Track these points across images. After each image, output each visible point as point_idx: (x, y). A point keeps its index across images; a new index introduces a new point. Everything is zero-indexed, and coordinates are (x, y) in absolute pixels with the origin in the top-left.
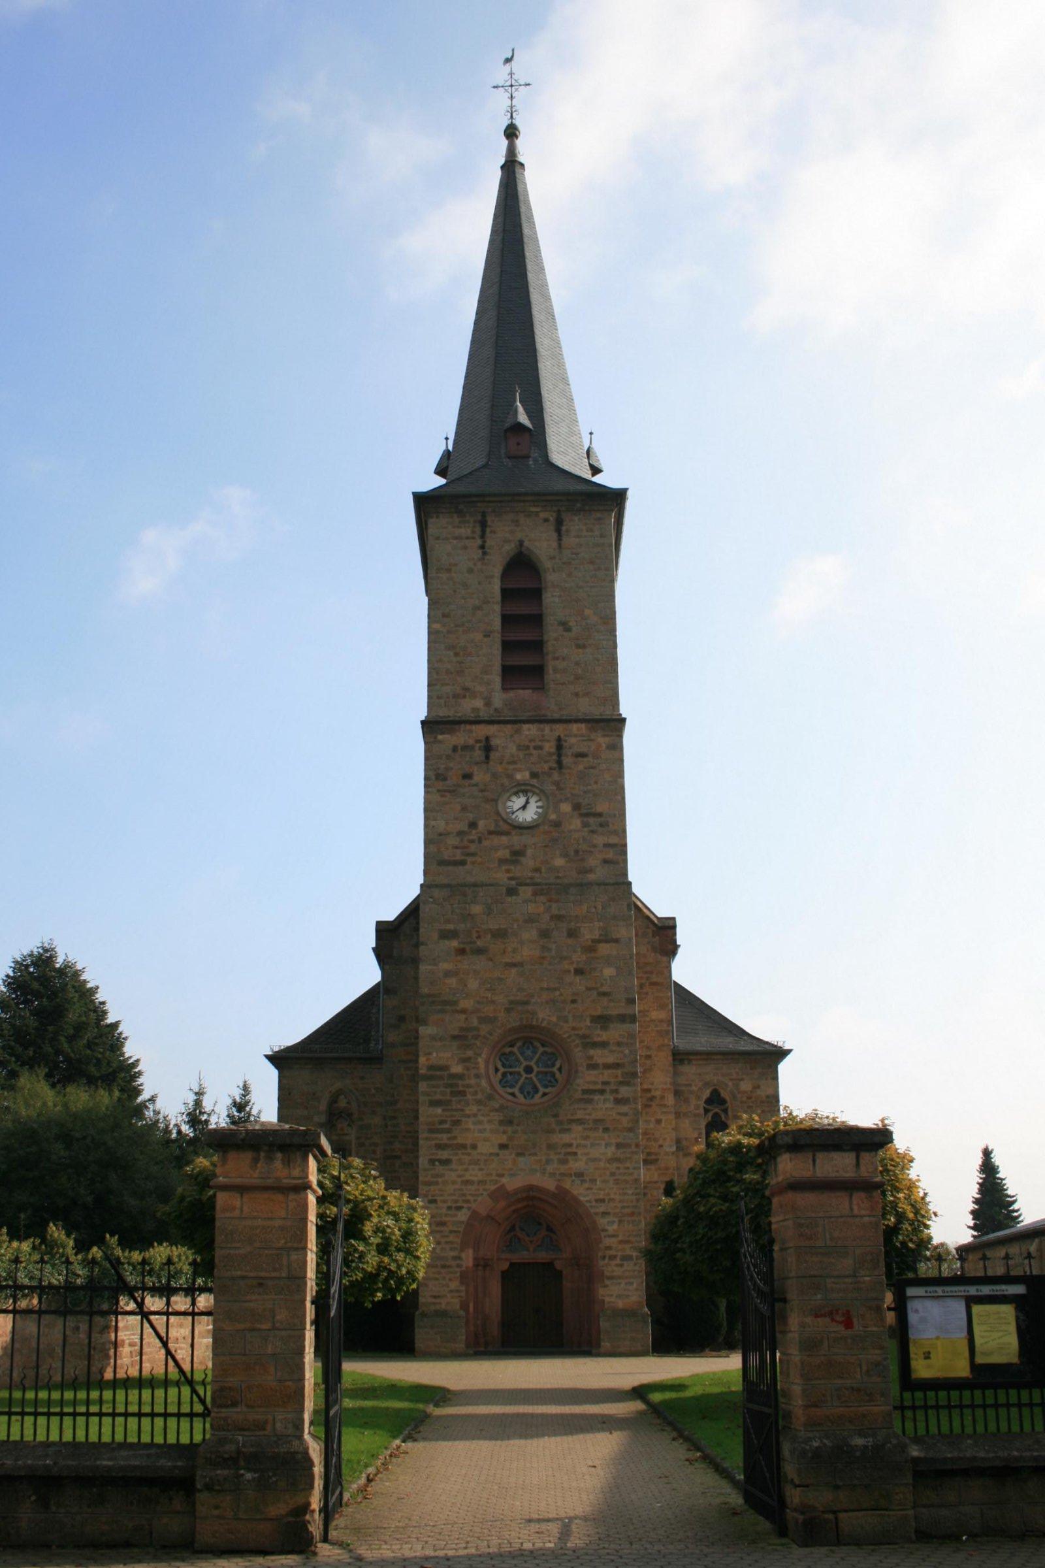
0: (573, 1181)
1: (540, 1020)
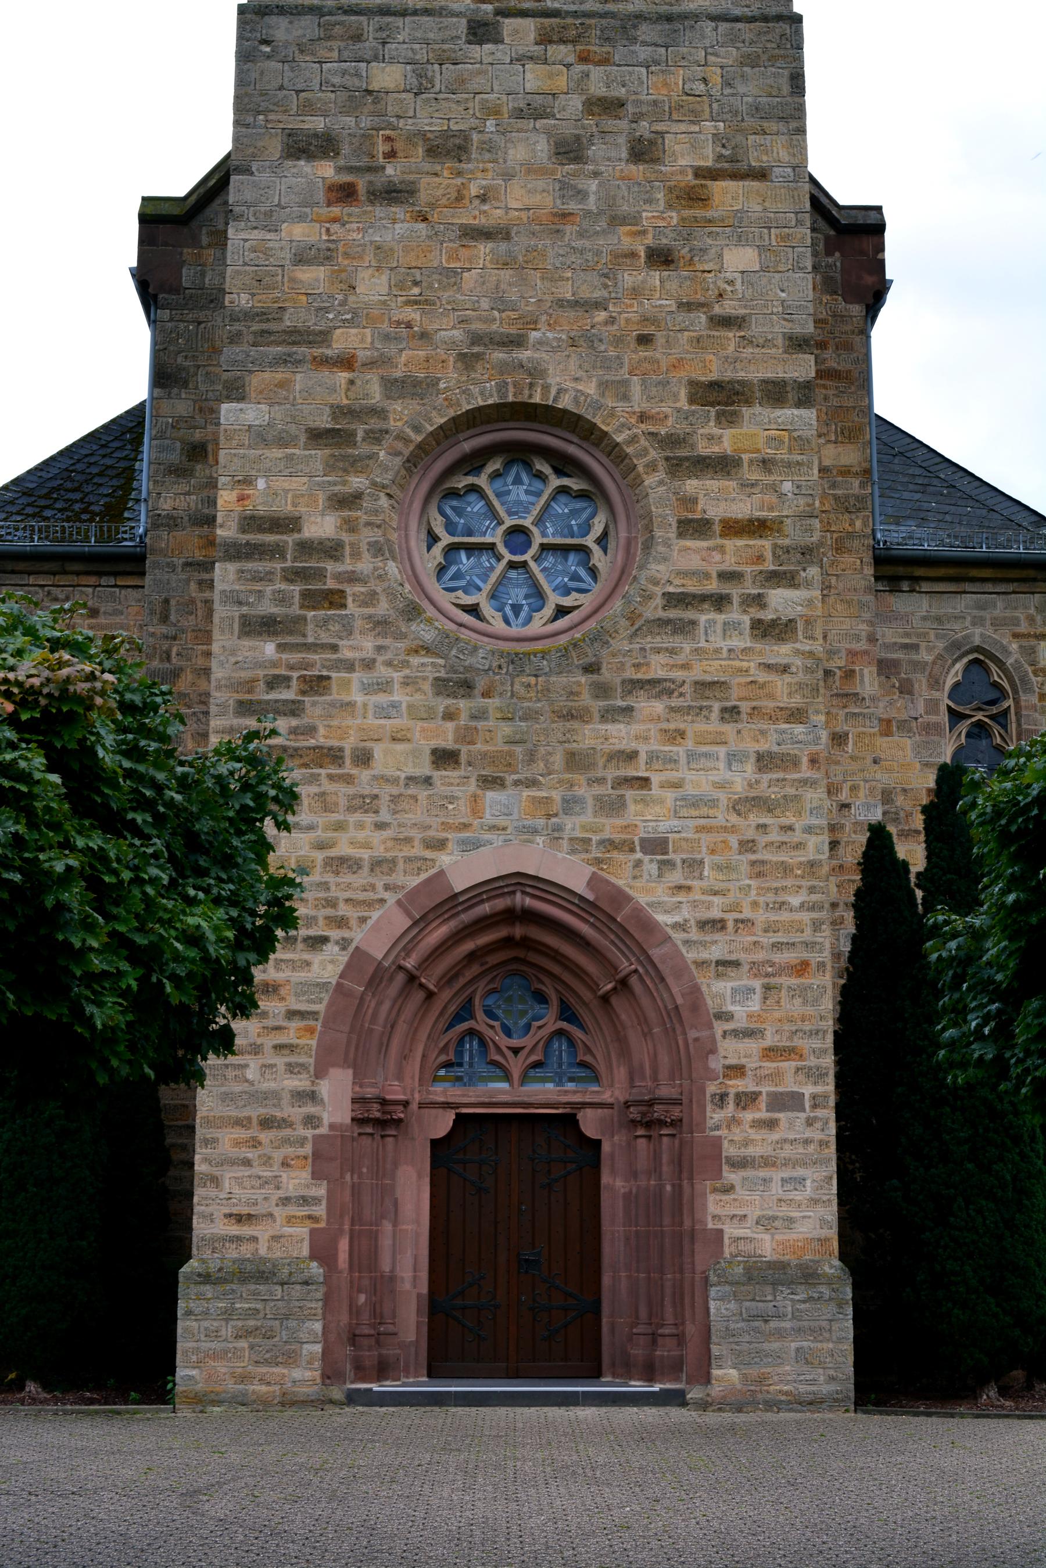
0: (638, 864)
1: (553, 392)
